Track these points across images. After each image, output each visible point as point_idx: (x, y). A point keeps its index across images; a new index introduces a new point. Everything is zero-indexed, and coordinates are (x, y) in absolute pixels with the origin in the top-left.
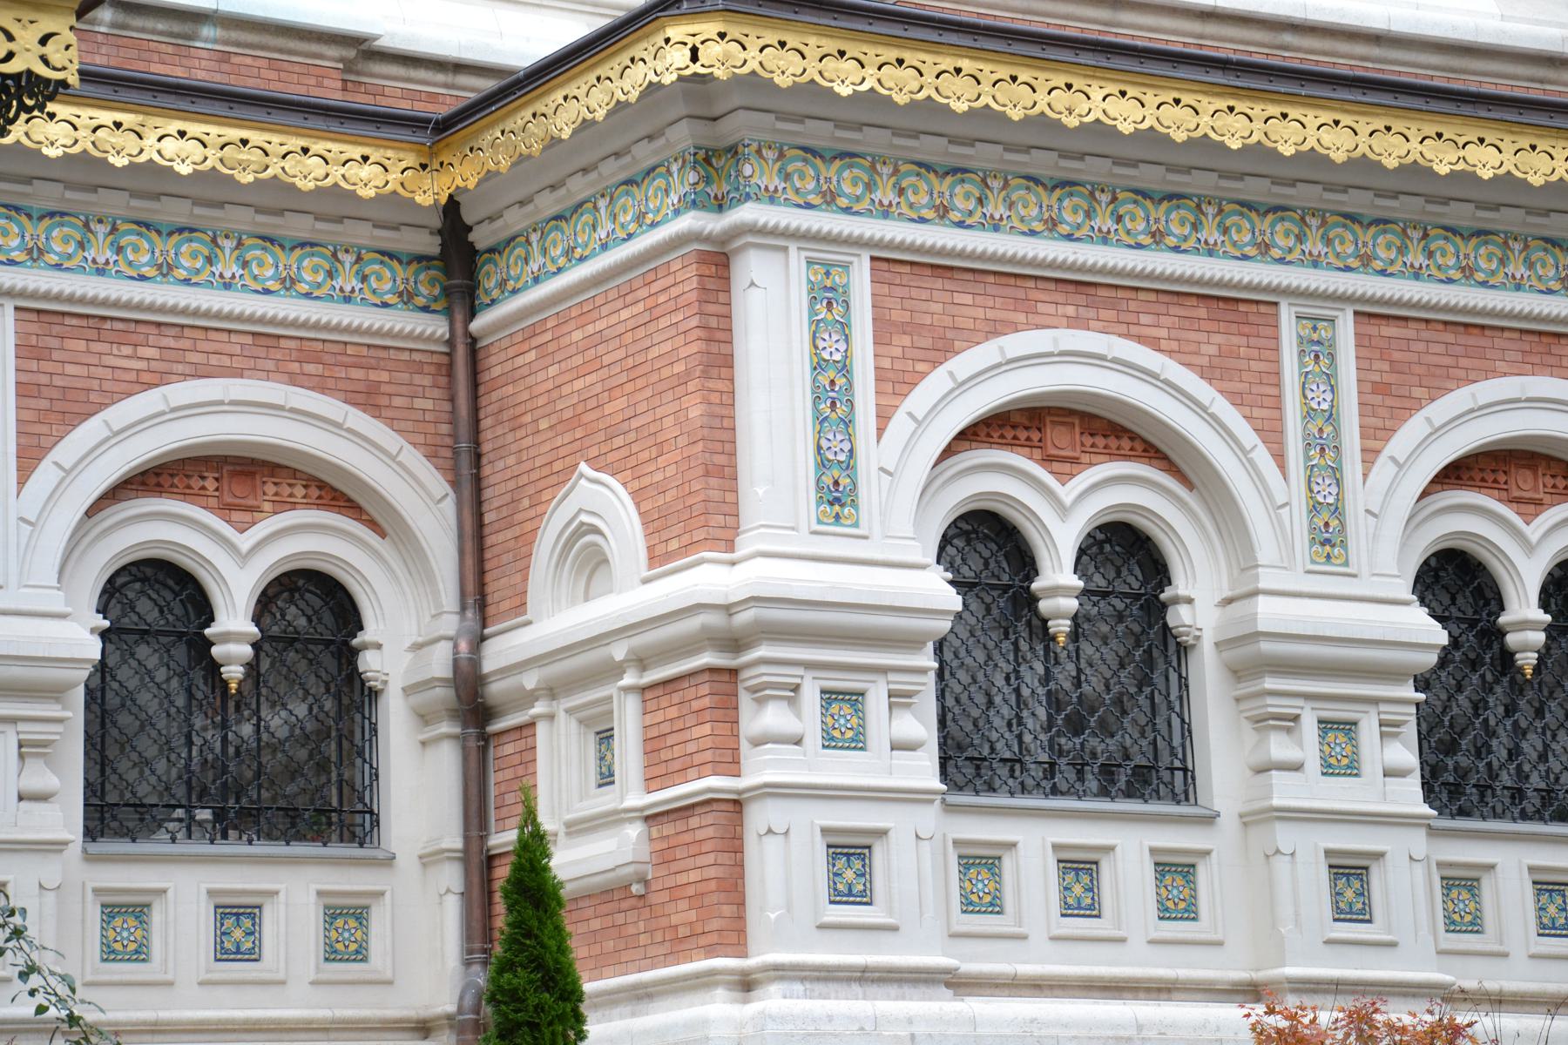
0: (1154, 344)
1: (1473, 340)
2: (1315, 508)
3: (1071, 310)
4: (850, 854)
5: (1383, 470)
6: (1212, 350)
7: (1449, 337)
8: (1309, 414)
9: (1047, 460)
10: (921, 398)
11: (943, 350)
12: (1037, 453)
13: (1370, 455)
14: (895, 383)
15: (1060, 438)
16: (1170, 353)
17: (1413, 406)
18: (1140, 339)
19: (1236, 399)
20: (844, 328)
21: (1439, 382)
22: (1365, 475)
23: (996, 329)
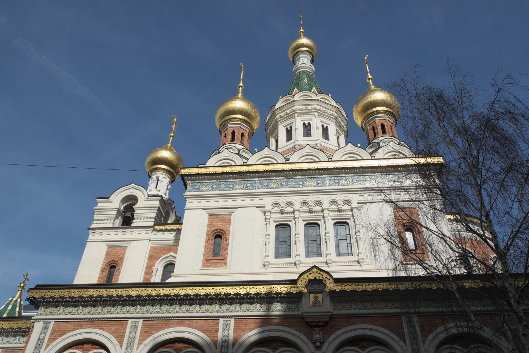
0: (103, 329)
8: (130, 338)
11: (64, 334)
13: (140, 344)
14: (51, 340)
15: (86, 346)
16: (106, 331)
17: (151, 334)
18: (101, 329)
19: (116, 337)
22: (138, 348)
23: (74, 330)
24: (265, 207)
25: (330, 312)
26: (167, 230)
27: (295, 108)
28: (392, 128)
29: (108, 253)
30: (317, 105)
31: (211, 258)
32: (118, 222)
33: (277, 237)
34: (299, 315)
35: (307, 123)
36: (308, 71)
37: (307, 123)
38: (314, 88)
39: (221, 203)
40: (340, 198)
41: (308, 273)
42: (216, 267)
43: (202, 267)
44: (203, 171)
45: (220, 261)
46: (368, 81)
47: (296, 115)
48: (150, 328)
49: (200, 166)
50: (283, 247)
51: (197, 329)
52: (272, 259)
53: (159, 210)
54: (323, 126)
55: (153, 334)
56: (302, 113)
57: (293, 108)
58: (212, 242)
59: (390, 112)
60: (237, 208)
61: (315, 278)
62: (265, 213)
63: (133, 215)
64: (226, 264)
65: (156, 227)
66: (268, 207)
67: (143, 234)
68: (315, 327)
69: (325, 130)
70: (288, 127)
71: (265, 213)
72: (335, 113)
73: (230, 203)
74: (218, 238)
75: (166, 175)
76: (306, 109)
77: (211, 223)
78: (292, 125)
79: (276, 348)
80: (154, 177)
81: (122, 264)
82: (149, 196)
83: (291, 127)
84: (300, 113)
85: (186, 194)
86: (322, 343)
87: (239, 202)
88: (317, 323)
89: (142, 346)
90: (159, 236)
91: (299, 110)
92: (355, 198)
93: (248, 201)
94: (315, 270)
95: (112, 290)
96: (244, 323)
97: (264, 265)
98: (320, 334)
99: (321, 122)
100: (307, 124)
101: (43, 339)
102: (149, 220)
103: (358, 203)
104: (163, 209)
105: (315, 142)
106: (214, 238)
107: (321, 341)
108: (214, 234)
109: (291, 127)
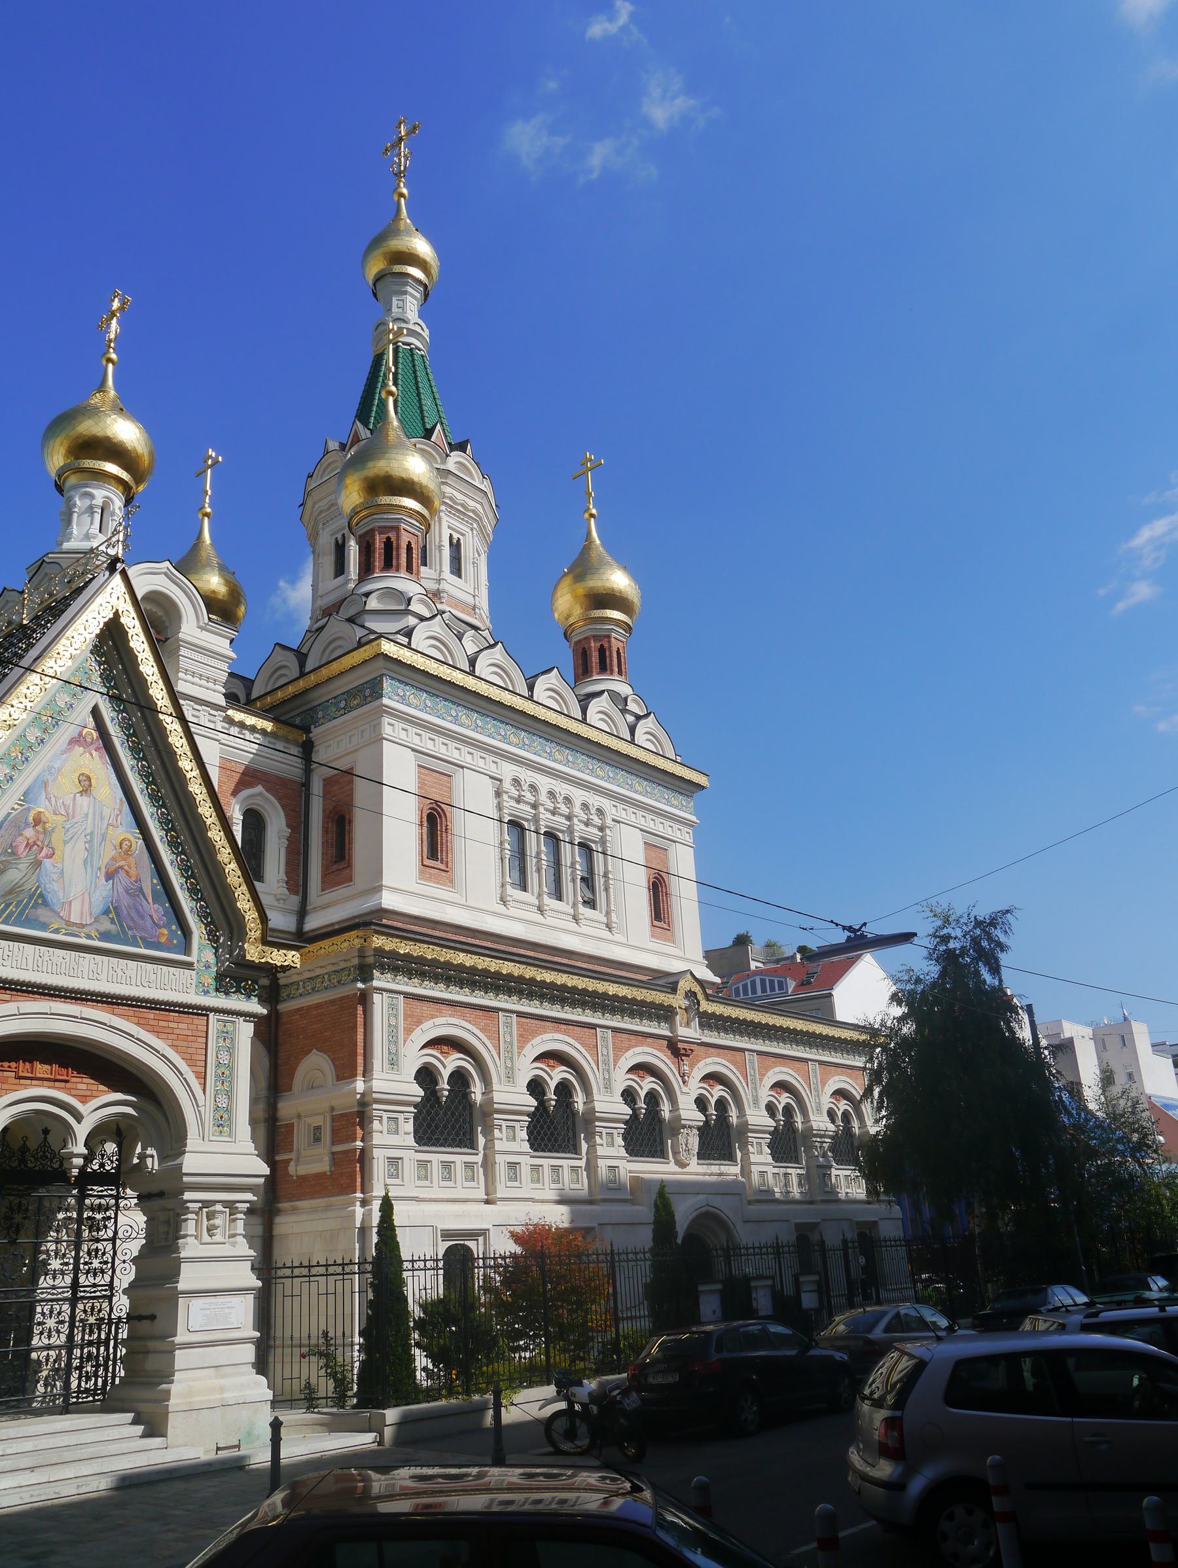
1: (543, 1023)
4: (394, 1161)
5: (522, 1058)
7: (537, 1022)
9: (442, 1053)
10: (414, 1036)
11: (419, 1022)
14: (409, 1031)
19: (489, 1038)
20: (396, 1016)
21: (535, 1033)
30: (481, 504)
37: (456, 536)
45: (443, 874)
64: (452, 881)
65: (230, 712)
66: (507, 785)
76: (462, 505)
99: (449, 527)
101: (396, 1027)
103: (614, 820)
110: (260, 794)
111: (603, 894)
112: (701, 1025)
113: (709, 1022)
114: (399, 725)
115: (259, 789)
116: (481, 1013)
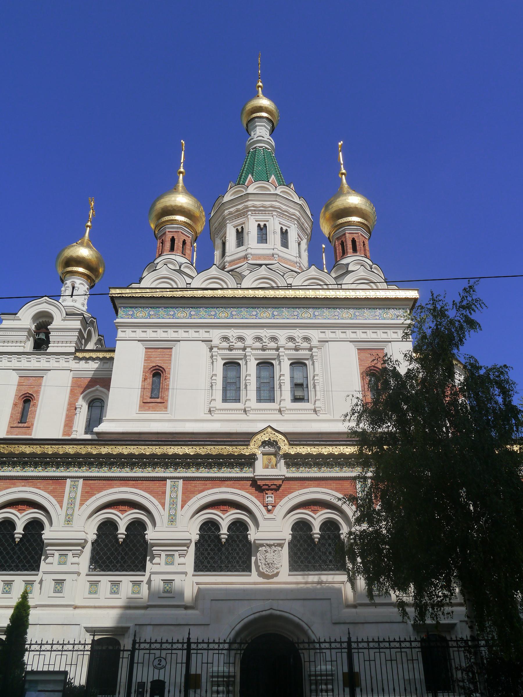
0: (39, 488)
2: (67, 515)
3: (23, 484)
6: (52, 488)
7: (104, 482)
8: (70, 498)
12: (17, 509)
13: (81, 504)
16: (42, 490)
18: (37, 488)
19: (54, 497)
21: (100, 490)
22: (79, 508)
24: (211, 341)
25: (284, 476)
26: (91, 359)
27: (249, 203)
28: (364, 245)
29: (20, 385)
30: (276, 201)
31: (149, 400)
32: (29, 346)
33: (225, 378)
34: (252, 478)
35: (262, 224)
36: (266, 148)
37: (262, 224)
38: (273, 176)
39: (160, 334)
40: (298, 333)
41: (262, 434)
42: (155, 411)
43: (139, 411)
44: (138, 293)
45: (160, 405)
46: (340, 176)
47: (250, 213)
48: (91, 488)
49: (134, 285)
50: (232, 390)
51: (143, 490)
52: (219, 403)
53: (80, 332)
54: (281, 228)
55: (95, 494)
56: (257, 211)
57: (246, 204)
58: (150, 380)
59: (363, 223)
60: (179, 341)
61: (270, 439)
62: (211, 349)
63: (48, 337)
64: (166, 408)
65: (78, 354)
66: (216, 342)
67: (62, 363)
68: (268, 490)
69: (284, 234)
70: (239, 228)
71: (211, 349)
72: (297, 213)
73: (171, 334)
74: (157, 375)
75: (83, 281)
76: (262, 207)
77: (148, 358)
78: (243, 225)
79: (227, 511)
80: (69, 283)
81: (38, 398)
82: (67, 314)
83: (242, 228)
84: (255, 210)
85: (118, 320)
86: (274, 506)
87: (181, 334)
88: (270, 487)
89: (84, 506)
90: (83, 365)
91: (253, 206)
92: (315, 335)
93: (192, 333)
94: (269, 430)
95: (46, 446)
96: (193, 485)
97: (210, 411)
98: (272, 497)
100: (262, 226)
102: (68, 345)
103: (319, 341)
104: (85, 330)
105: (270, 252)
106: (151, 376)
107: (273, 505)
108: (152, 371)
109: (242, 228)
110: (97, 390)
111: (313, 390)
112: (288, 465)
113: (292, 461)
114: (129, 331)
115: (98, 386)
116: (51, 482)
